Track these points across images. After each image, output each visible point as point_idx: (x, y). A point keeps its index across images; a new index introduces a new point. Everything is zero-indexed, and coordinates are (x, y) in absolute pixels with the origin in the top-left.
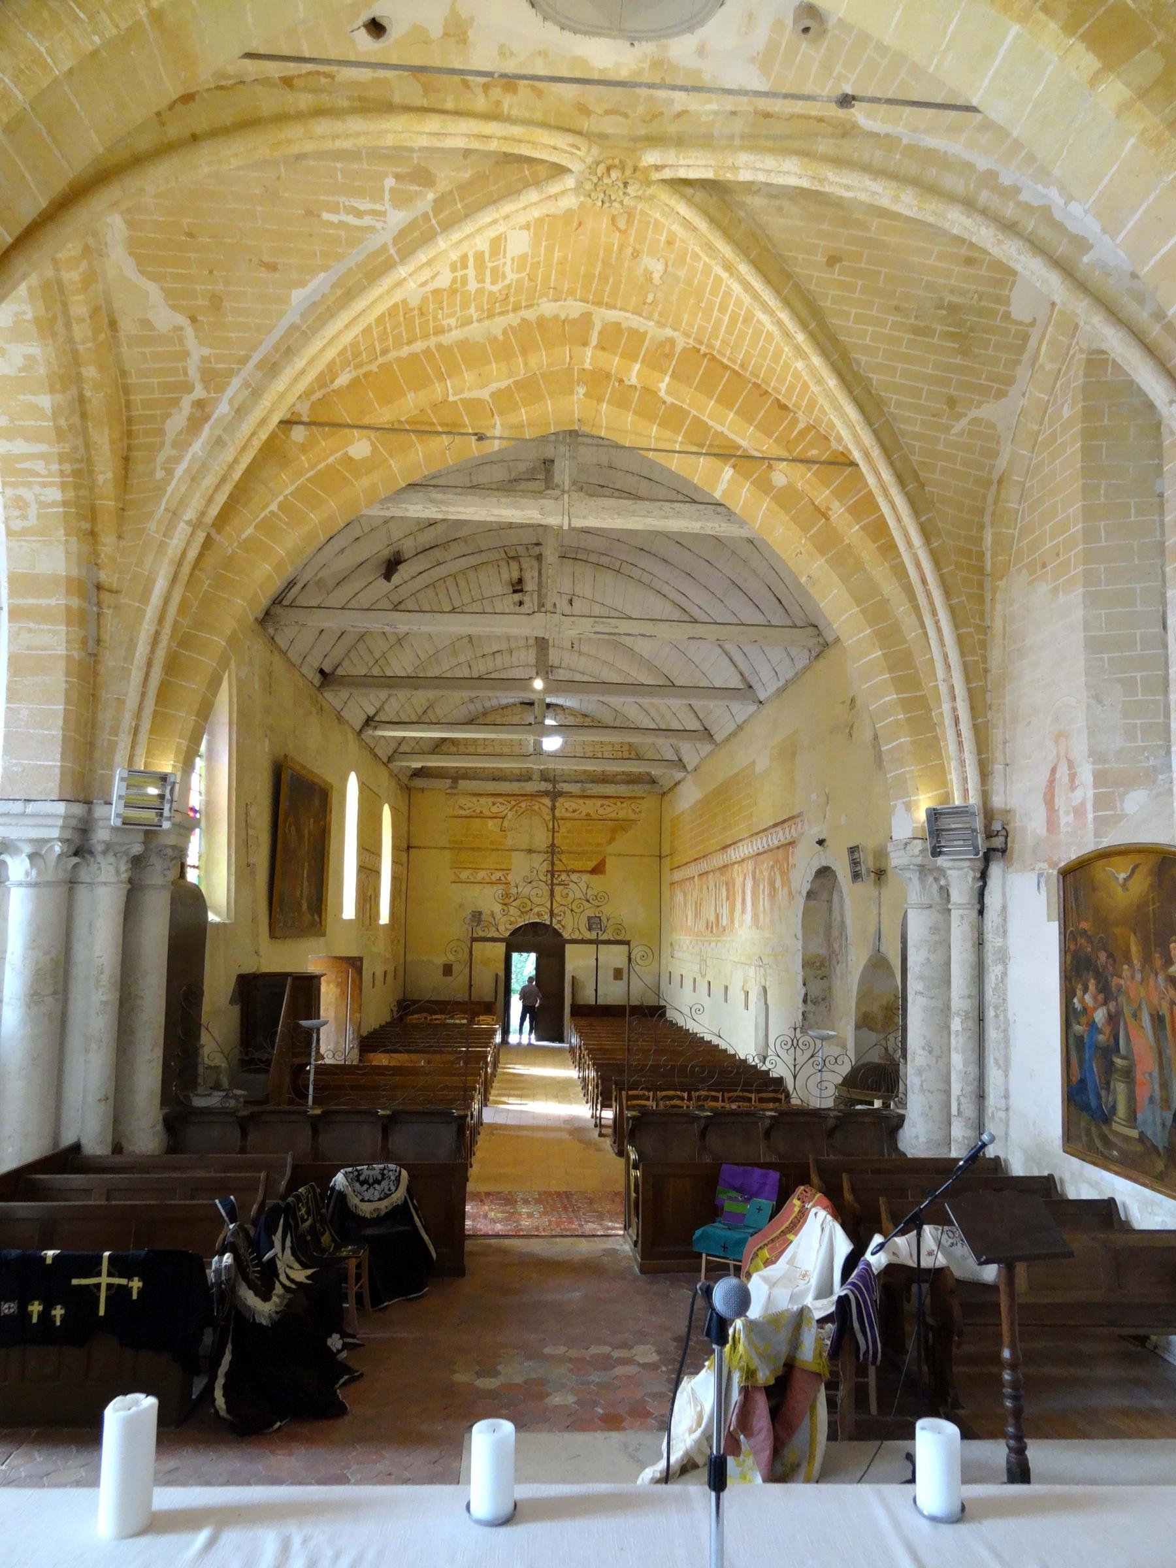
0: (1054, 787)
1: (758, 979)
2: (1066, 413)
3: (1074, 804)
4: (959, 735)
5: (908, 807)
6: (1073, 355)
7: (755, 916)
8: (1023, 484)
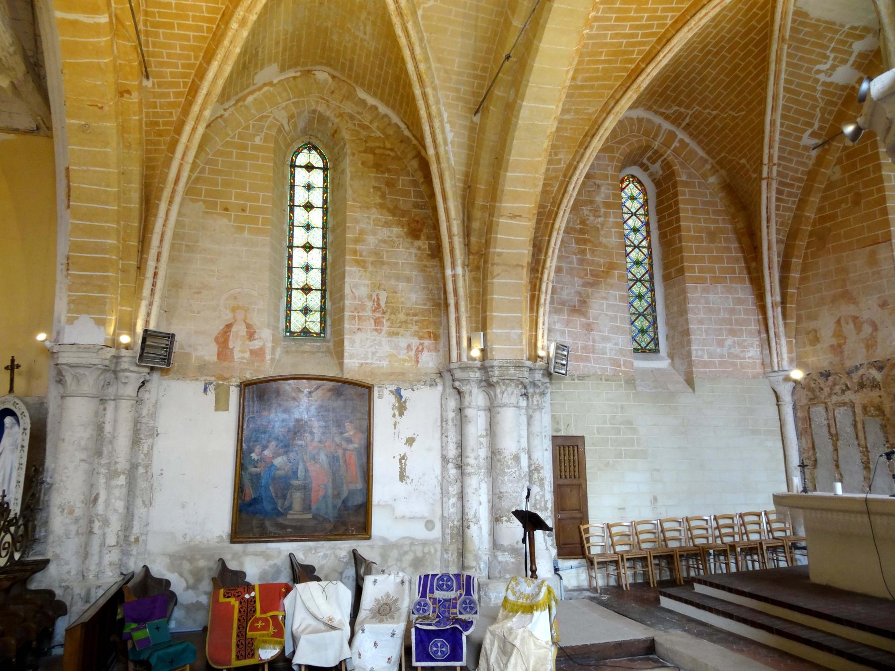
0: (229, 336)
2: (258, 140)
3: (251, 348)
4: (154, 285)
5: (101, 323)
6: (268, 117)
8: (209, 154)
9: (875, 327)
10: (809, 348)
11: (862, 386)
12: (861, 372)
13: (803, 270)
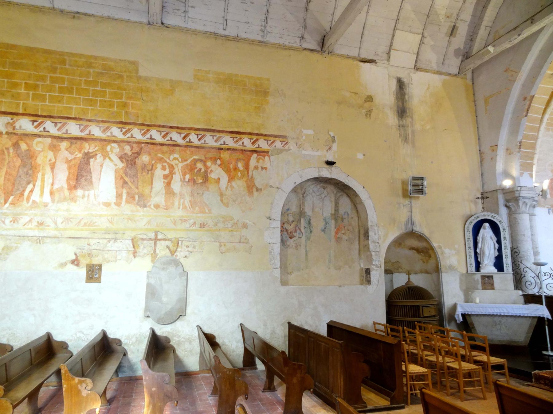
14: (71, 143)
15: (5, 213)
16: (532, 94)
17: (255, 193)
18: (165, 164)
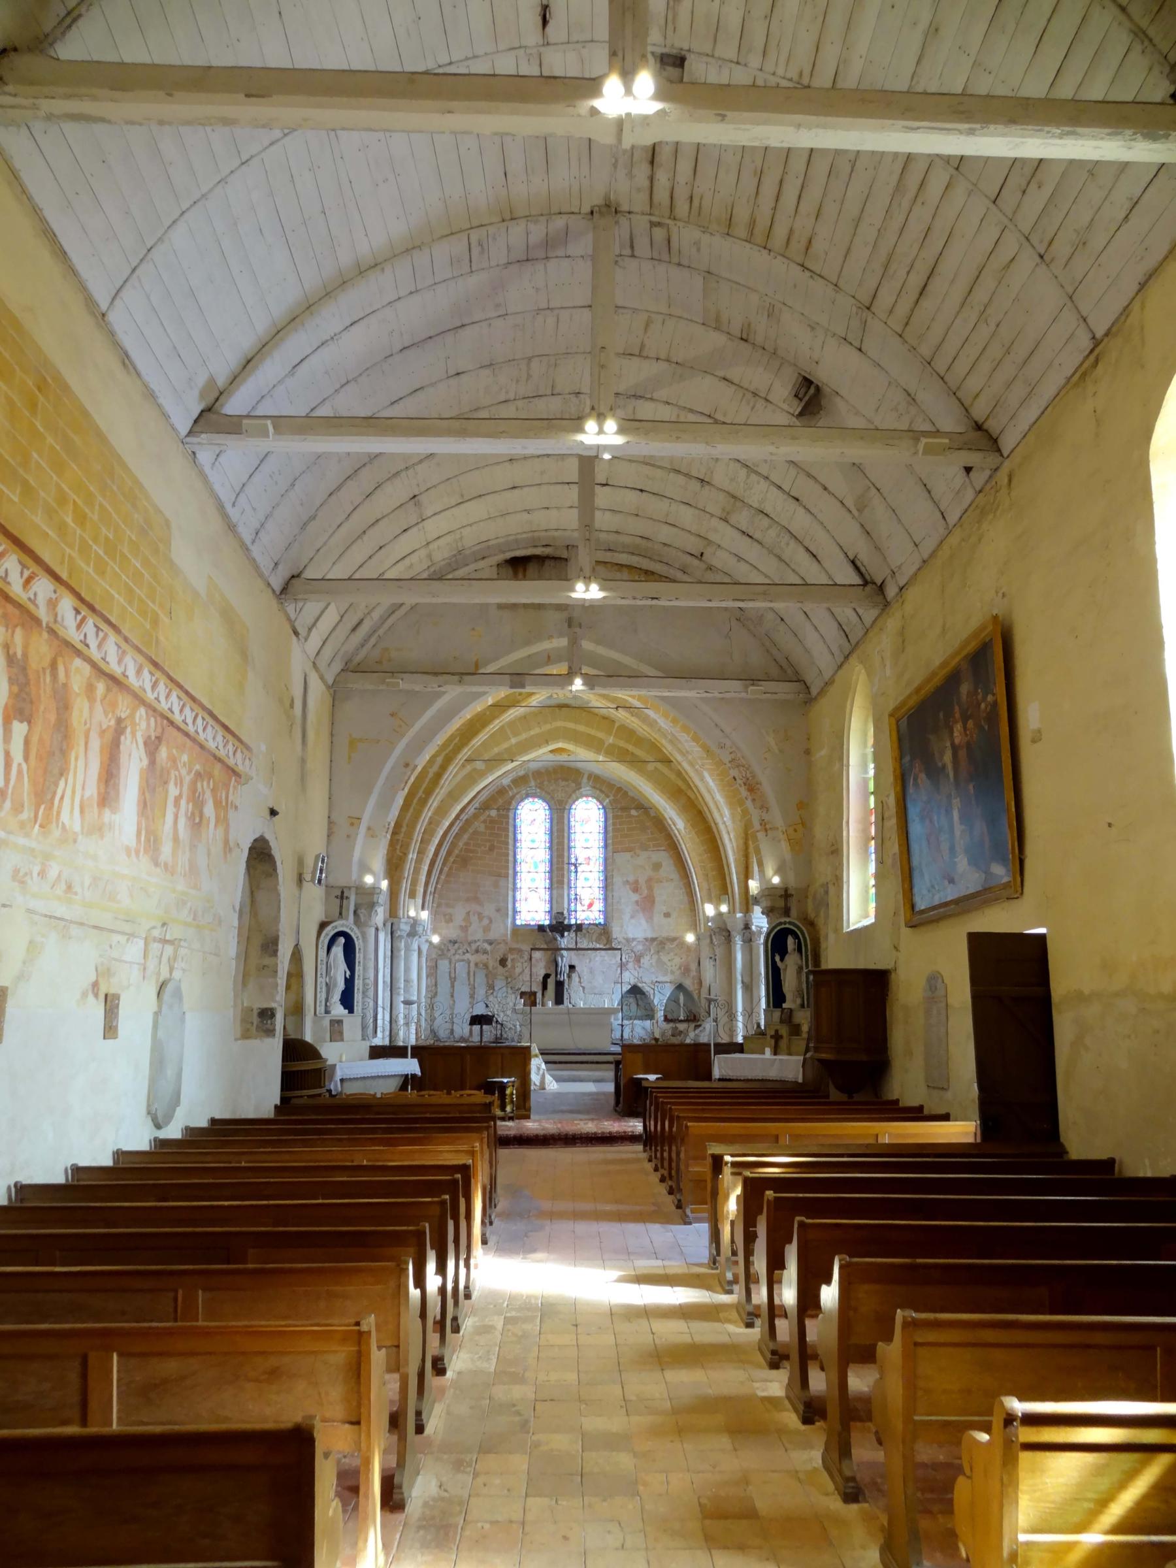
1: (152, 965)
7: (150, 841)
9: (491, 921)
10: (443, 924)
11: (477, 951)
12: (478, 944)
13: (448, 875)
14: (108, 690)
15: (32, 850)
16: (416, 763)
17: (228, 855)
18: (177, 773)
